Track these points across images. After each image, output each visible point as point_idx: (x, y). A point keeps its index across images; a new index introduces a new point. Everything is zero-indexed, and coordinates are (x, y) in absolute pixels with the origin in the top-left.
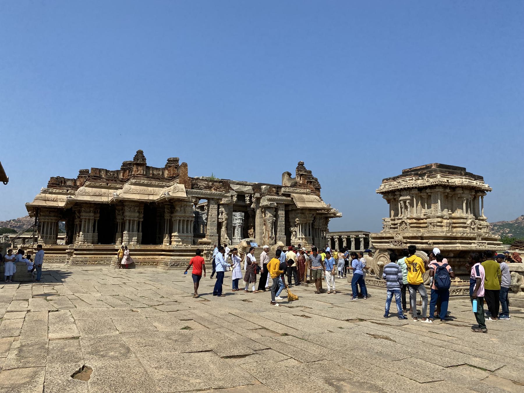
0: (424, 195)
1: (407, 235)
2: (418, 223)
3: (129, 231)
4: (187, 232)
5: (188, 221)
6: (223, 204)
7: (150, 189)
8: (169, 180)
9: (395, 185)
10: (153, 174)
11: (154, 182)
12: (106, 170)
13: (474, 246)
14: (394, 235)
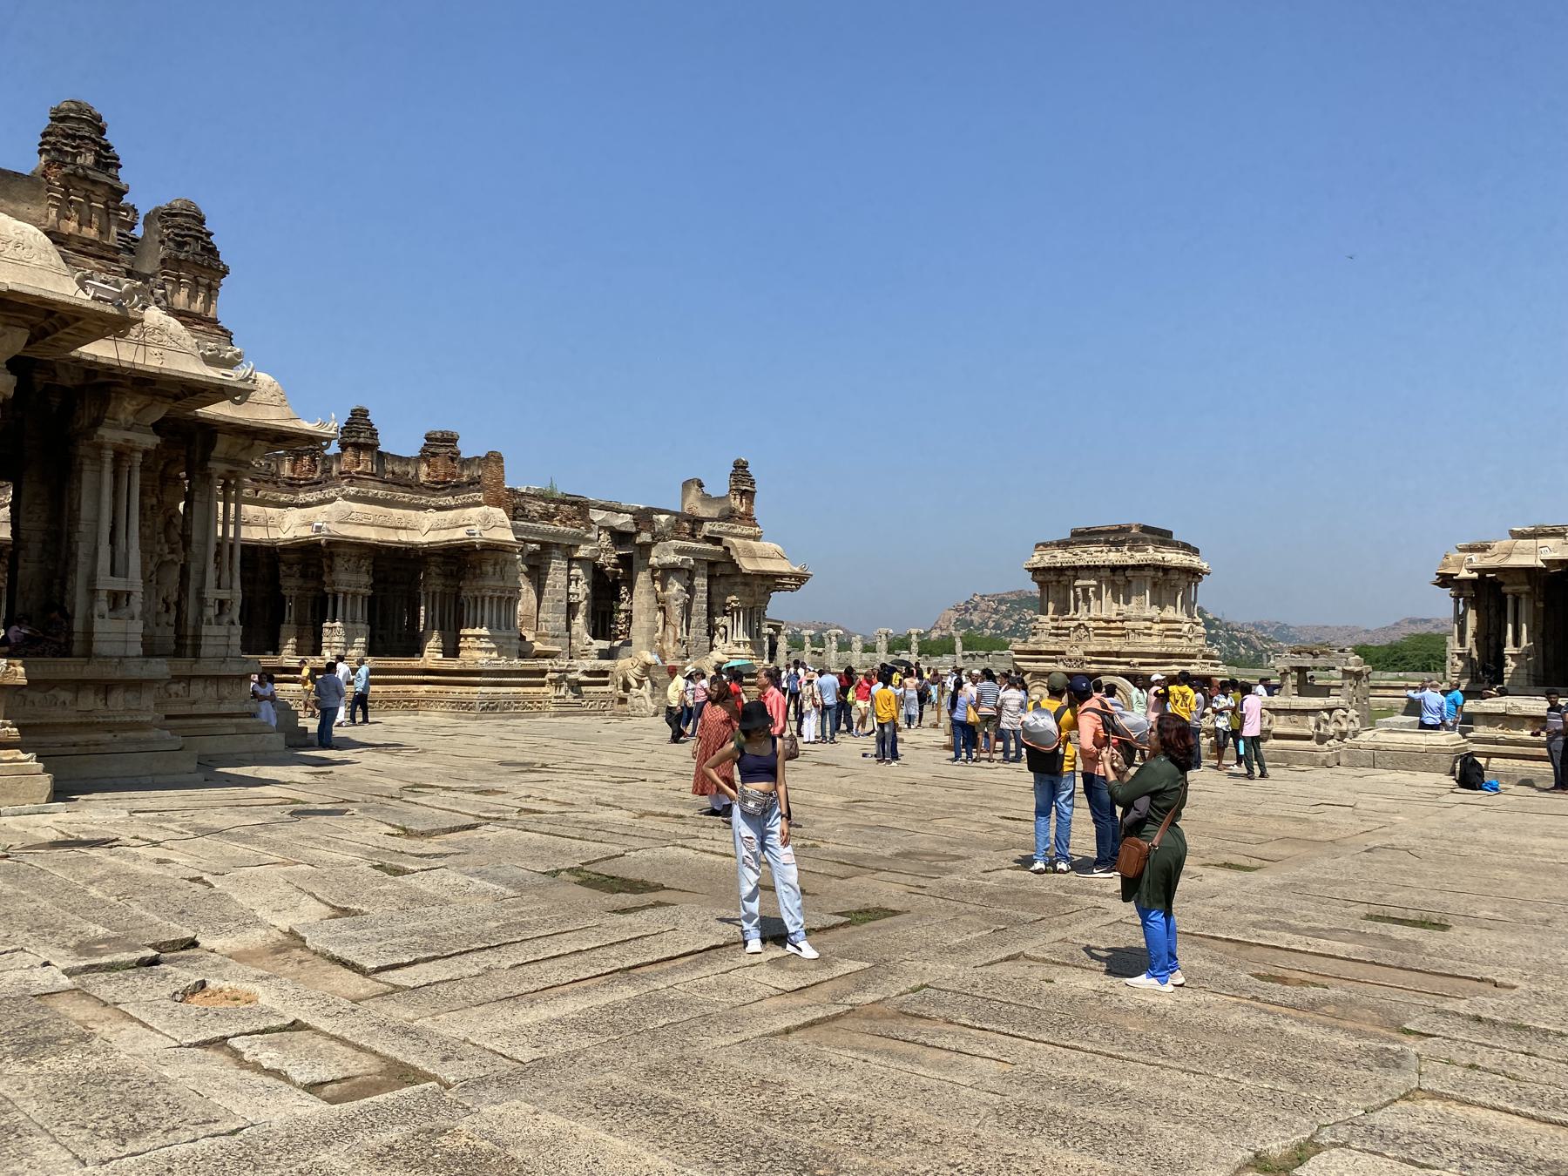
0: (1120, 579)
1: (1092, 648)
2: (1107, 628)
6: (579, 560)
7: (397, 513)
8: (435, 489)
9: (1062, 558)
11: (400, 495)
14: (1066, 648)
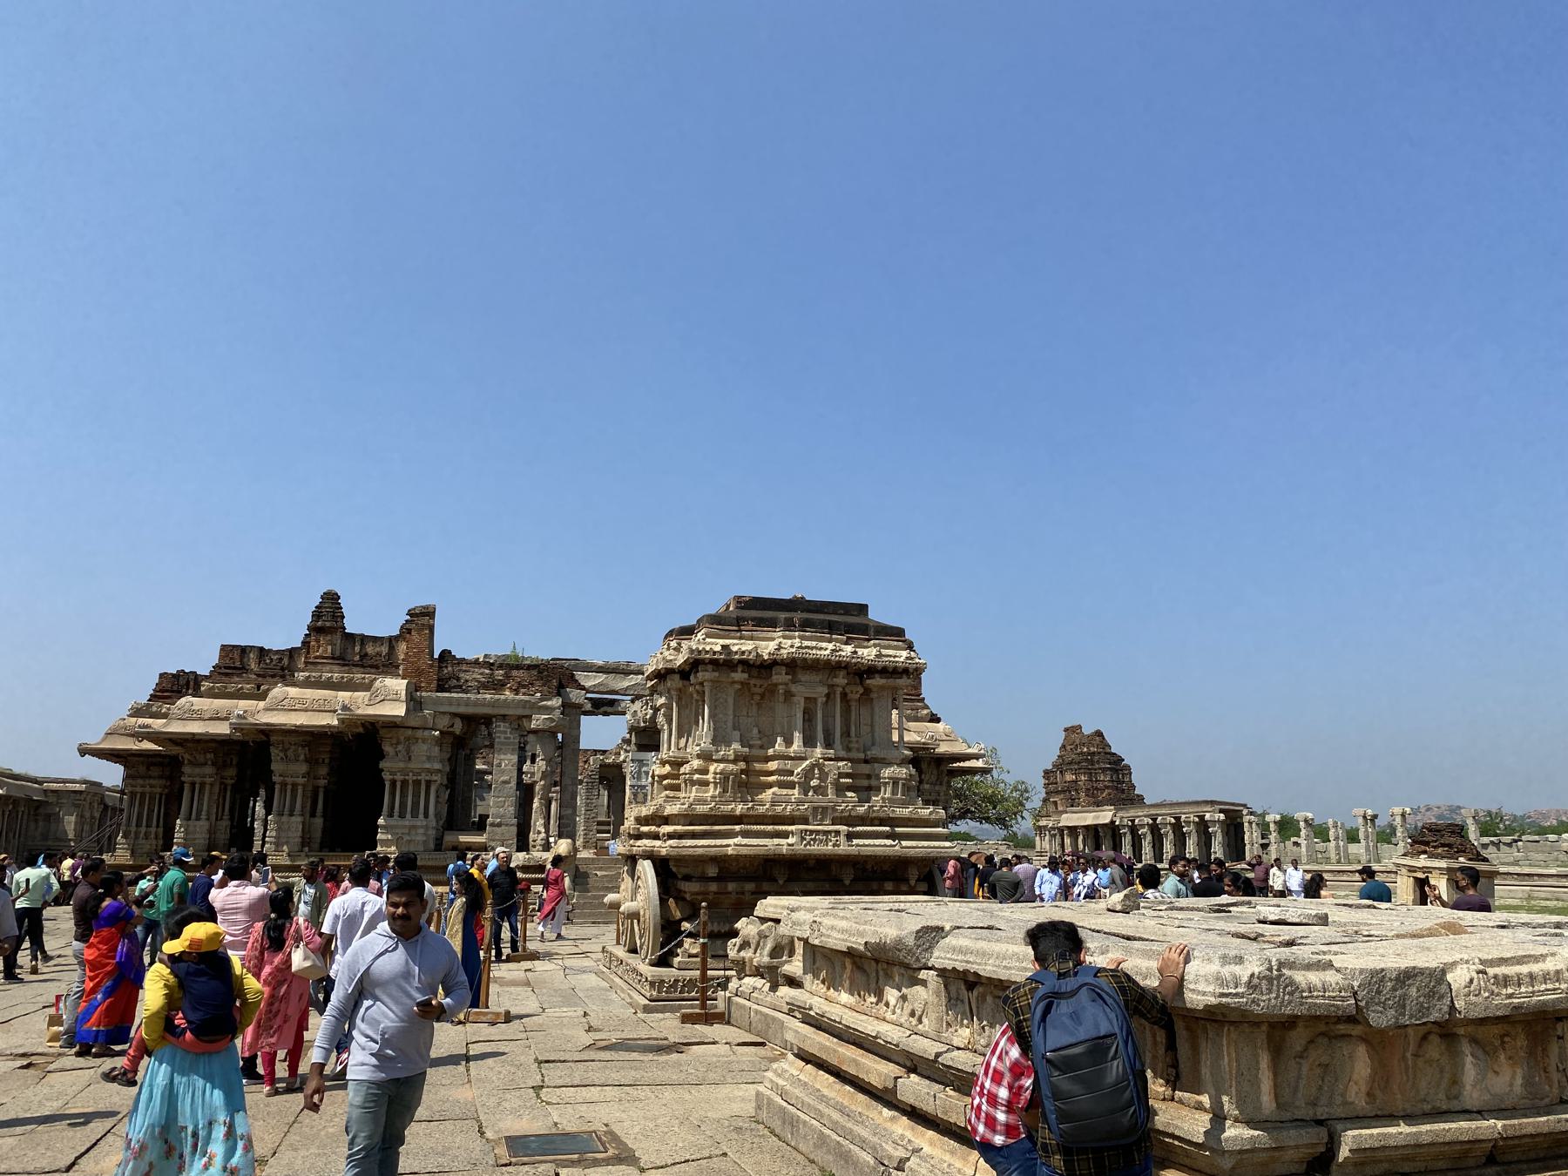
3: (281, 814)
4: (415, 815)
5: (417, 783)
6: (535, 732)
10: (364, 656)
12: (262, 649)
13: (789, 844)
